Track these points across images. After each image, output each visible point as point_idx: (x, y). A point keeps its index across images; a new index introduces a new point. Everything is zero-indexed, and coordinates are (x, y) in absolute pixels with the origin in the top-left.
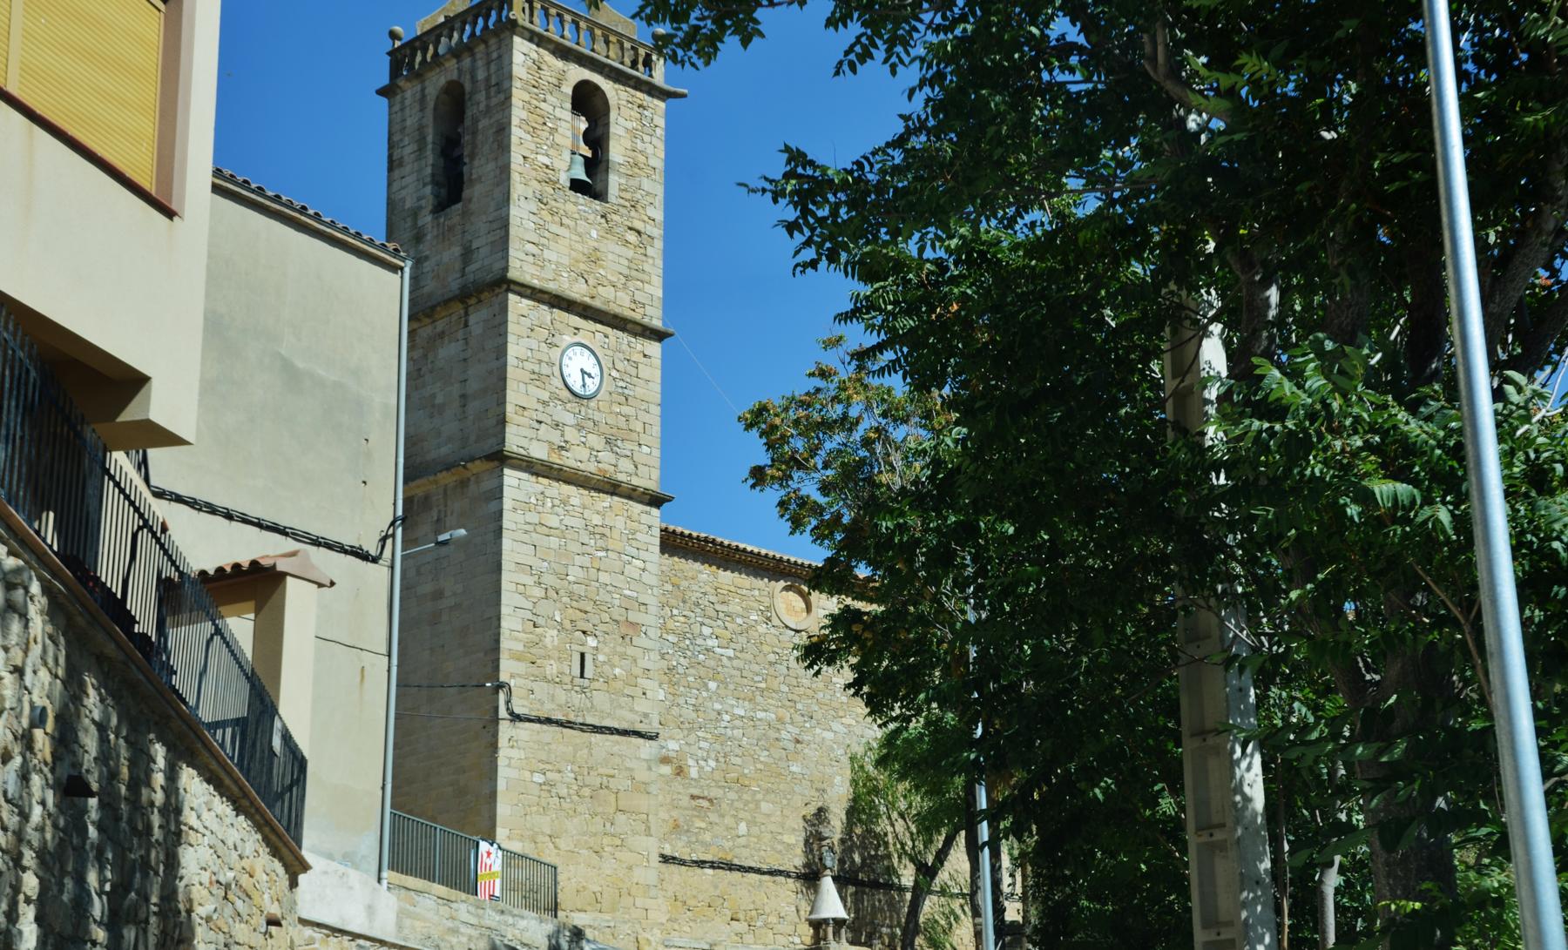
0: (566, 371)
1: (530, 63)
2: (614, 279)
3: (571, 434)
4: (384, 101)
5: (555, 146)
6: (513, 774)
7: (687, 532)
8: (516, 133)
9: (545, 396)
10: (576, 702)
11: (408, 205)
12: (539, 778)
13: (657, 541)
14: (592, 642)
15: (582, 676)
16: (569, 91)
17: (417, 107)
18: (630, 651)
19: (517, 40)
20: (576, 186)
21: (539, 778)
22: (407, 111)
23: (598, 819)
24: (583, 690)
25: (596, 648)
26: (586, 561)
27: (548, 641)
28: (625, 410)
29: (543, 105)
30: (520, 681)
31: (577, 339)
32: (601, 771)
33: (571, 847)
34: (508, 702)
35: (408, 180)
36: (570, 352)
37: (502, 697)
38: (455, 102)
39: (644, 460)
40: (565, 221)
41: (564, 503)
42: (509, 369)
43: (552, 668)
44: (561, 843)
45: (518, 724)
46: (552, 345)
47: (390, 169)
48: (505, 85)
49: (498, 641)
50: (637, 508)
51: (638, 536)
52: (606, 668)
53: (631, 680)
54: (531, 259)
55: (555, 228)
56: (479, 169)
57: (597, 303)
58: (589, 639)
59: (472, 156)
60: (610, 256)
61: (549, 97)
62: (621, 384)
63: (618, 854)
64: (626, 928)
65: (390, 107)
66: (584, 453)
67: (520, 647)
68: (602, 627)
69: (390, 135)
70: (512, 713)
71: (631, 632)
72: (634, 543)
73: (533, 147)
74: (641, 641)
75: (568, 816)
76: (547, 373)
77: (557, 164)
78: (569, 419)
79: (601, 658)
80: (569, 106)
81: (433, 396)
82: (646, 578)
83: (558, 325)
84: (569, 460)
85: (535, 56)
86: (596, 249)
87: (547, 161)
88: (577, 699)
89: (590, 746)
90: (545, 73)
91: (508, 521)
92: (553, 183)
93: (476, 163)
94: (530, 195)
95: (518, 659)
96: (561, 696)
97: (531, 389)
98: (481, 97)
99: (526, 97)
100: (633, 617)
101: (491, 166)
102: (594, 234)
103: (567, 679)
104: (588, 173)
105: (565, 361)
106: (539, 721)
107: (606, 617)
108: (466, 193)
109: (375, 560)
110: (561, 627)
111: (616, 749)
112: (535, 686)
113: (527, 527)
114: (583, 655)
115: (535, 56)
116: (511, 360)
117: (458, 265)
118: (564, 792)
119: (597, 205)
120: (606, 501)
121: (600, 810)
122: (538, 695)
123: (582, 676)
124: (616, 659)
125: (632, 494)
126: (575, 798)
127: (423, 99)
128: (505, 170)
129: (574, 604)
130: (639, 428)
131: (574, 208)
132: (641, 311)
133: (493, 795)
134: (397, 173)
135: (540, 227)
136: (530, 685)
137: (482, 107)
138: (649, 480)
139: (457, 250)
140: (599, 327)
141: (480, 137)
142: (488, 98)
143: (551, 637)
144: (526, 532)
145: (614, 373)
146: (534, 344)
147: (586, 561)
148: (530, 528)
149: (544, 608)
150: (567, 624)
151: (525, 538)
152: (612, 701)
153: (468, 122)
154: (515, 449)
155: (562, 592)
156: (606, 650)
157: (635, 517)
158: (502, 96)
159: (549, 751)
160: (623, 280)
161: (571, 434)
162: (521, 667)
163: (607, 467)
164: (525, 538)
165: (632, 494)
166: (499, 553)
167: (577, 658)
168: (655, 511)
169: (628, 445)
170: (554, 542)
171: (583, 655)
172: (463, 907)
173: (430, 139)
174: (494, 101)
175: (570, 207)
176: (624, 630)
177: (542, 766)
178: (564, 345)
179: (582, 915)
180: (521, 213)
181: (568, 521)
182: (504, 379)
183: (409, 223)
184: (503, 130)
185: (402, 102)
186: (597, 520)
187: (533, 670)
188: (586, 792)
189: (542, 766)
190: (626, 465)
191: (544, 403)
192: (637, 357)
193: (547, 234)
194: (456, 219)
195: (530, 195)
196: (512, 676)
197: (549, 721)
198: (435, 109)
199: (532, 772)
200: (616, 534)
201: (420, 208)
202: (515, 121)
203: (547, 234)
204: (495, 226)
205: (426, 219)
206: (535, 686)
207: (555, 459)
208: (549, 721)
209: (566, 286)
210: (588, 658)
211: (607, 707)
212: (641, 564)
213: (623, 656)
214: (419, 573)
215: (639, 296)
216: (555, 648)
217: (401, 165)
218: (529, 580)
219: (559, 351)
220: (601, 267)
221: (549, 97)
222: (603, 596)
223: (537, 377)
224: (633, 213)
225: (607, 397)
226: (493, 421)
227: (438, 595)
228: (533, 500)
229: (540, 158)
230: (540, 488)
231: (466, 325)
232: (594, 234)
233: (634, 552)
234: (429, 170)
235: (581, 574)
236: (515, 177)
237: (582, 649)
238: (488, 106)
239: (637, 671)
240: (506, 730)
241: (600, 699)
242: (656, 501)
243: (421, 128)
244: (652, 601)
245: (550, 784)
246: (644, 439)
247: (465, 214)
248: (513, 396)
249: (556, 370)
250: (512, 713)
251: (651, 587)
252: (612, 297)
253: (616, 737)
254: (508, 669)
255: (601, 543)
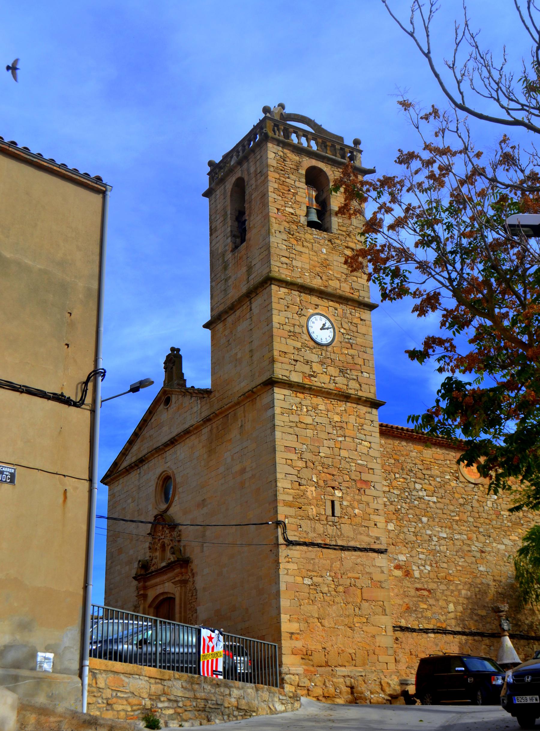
0: (311, 330)
1: (278, 158)
2: (339, 276)
3: (317, 367)
4: (207, 199)
5: (296, 202)
6: (290, 579)
7: (400, 427)
8: (272, 196)
9: (299, 345)
10: (330, 531)
11: (220, 251)
12: (307, 581)
13: (377, 430)
14: (338, 493)
15: (333, 515)
16: (304, 172)
17: (222, 197)
18: (364, 498)
19: (270, 145)
20: (311, 224)
21: (307, 581)
22: (218, 201)
23: (350, 606)
24: (334, 524)
25: (342, 497)
26: (331, 443)
27: (309, 494)
28: (351, 352)
29: (288, 180)
30: (292, 520)
31: (317, 311)
32: (350, 575)
33: (333, 625)
34: (284, 533)
35: (219, 237)
36: (313, 319)
37: (280, 531)
38: (240, 186)
39: (365, 381)
40: (305, 244)
41: (315, 408)
42: (275, 330)
43: (313, 511)
44: (326, 623)
45: (290, 547)
46: (301, 315)
47: (211, 235)
48: (265, 171)
49: (276, 495)
50: (363, 409)
51: (365, 427)
52: (349, 509)
53: (366, 517)
54: (285, 266)
55: (299, 248)
56: (253, 221)
57: (329, 290)
58: (337, 492)
59: (250, 216)
60: (335, 263)
61: (291, 176)
62: (347, 337)
63: (364, 628)
64: (373, 676)
65: (210, 201)
66: (326, 379)
67: (290, 498)
68: (345, 484)
69: (210, 216)
70: (286, 539)
71: (364, 486)
72: (362, 431)
73: (283, 203)
74: (371, 491)
75: (329, 605)
76: (299, 332)
77: (298, 212)
78: (314, 358)
79: (345, 503)
80: (304, 180)
81: (236, 354)
82: (372, 453)
83: (304, 304)
84: (316, 382)
85: (282, 154)
86: (326, 259)
87: (291, 210)
88: (331, 530)
89: (341, 560)
90: (288, 163)
91: (279, 420)
92: (297, 223)
93: (252, 218)
94: (282, 230)
95: (290, 507)
96: (320, 528)
97: (289, 341)
98: (253, 182)
99: (277, 176)
100: (365, 477)
101: (260, 217)
102: (324, 251)
103: (323, 518)
104: (319, 219)
105: (310, 324)
106: (305, 544)
107: (347, 478)
108: (247, 237)
109: (76, 405)
110: (317, 485)
111: (359, 561)
112: (302, 523)
113: (291, 424)
114: (333, 502)
115: (282, 154)
116: (275, 325)
117: (245, 278)
118: (325, 589)
119: (325, 235)
120: (342, 406)
121: (351, 600)
122: (304, 528)
123: (333, 515)
124: (356, 504)
125: (359, 401)
126: (333, 593)
127: (225, 193)
128: (267, 217)
129: (325, 470)
130: (361, 362)
131: (311, 237)
132: (357, 294)
133: (278, 594)
134: (214, 236)
135: (289, 248)
136: (299, 522)
137: (253, 187)
138: (369, 392)
139: (244, 269)
140: (331, 303)
141: (253, 203)
142: (256, 181)
143: (311, 492)
144: (291, 427)
145: (342, 330)
146: (290, 315)
147: (331, 443)
148: (294, 425)
149: (305, 473)
150: (321, 483)
151: (291, 431)
152: (354, 530)
153: (247, 197)
154: (281, 377)
155: (316, 464)
156: (348, 498)
157: (362, 416)
158: (263, 178)
159: (314, 564)
160: (344, 276)
161: (317, 367)
162: (291, 511)
163: (341, 386)
164: (291, 431)
165: (359, 401)
166: (274, 441)
167: (329, 504)
168: (375, 411)
169: (354, 373)
170: (309, 433)
171: (333, 502)
172: (178, 684)
173: (229, 212)
174: (259, 181)
175: (308, 236)
176: (359, 485)
177: (310, 574)
178: (309, 315)
179: (343, 669)
180: (278, 241)
181: (318, 419)
182: (272, 336)
183: (221, 261)
184: (264, 196)
185: (215, 197)
186: (337, 418)
187: (300, 512)
188: (341, 589)
189: (310, 574)
190: (353, 384)
191: (298, 349)
192: (355, 321)
193: (294, 252)
194: (243, 252)
195: (282, 230)
196: (286, 517)
197: (312, 544)
198: (231, 196)
199: (303, 578)
200: (350, 426)
201: (226, 251)
202: (271, 189)
203: (294, 252)
204: (262, 250)
205: (229, 256)
206: (302, 523)
207: (307, 381)
208: (312, 544)
209: (308, 280)
210: (337, 504)
211: (351, 534)
212: (369, 445)
213: (360, 502)
214: (233, 459)
215: (355, 286)
216: (313, 498)
217: (216, 231)
218: (294, 457)
219: (306, 318)
220: (330, 269)
221: (291, 176)
222: (344, 464)
223: (293, 335)
224: (348, 239)
225: (339, 345)
226: (267, 363)
227: (243, 471)
228: (294, 408)
229: (287, 209)
230: (298, 400)
231: (251, 310)
232: (324, 251)
233: (363, 437)
234: (229, 229)
235: (328, 452)
236: (273, 220)
237: (331, 498)
238: (256, 185)
239: (369, 511)
240: (283, 551)
241: (347, 529)
242: (375, 404)
243: (224, 209)
244: (377, 467)
245: (316, 585)
246: (364, 369)
247: (247, 248)
248: (278, 346)
249: (305, 329)
250: (286, 539)
251: (376, 458)
252: (338, 287)
253: (358, 553)
254: (283, 512)
255: (340, 432)
